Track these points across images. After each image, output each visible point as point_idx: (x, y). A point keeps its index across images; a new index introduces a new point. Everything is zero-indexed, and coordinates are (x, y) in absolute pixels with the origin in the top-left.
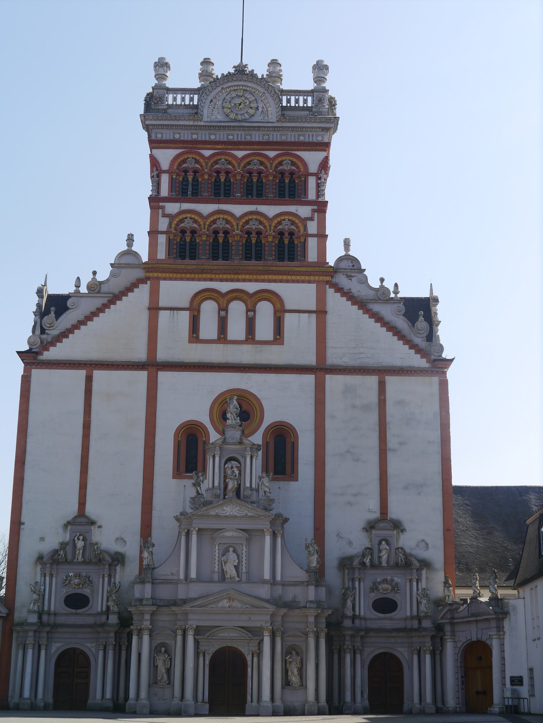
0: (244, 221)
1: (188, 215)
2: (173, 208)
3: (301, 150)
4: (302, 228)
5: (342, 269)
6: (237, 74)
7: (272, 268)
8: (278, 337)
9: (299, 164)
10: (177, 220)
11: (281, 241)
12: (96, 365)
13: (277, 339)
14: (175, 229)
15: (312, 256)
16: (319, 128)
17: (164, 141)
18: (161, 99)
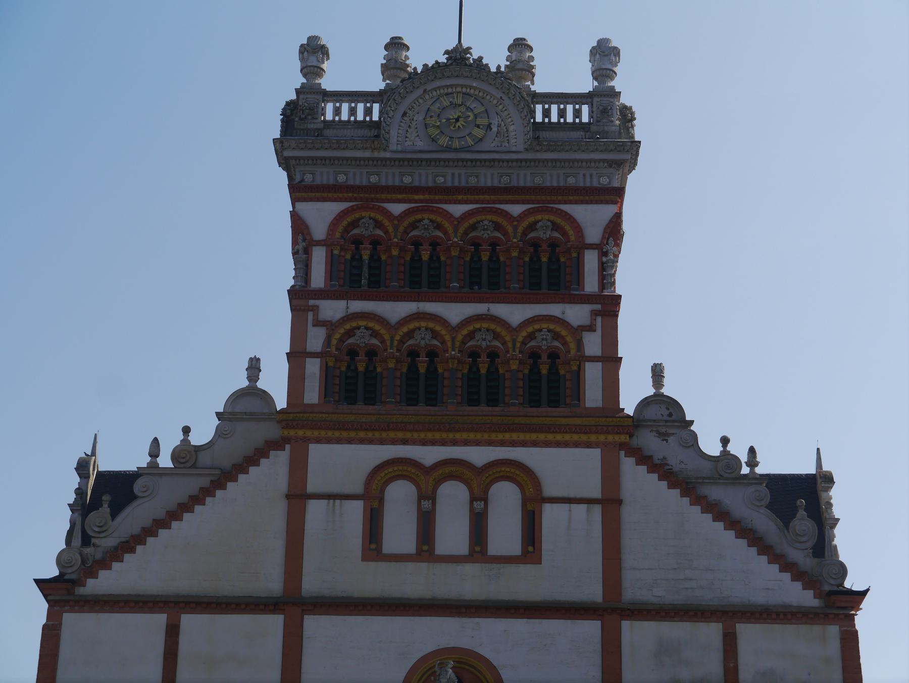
0: (465, 332)
1: (362, 323)
2: (333, 309)
3: (571, 202)
4: (572, 346)
5: (650, 421)
6: (451, 64)
7: (517, 420)
8: (530, 549)
9: (567, 228)
10: (342, 331)
11: (535, 369)
12: (187, 603)
13: (528, 552)
14: (337, 349)
15: (593, 396)
16: (604, 161)
17: (317, 186)
18: (315, 111)
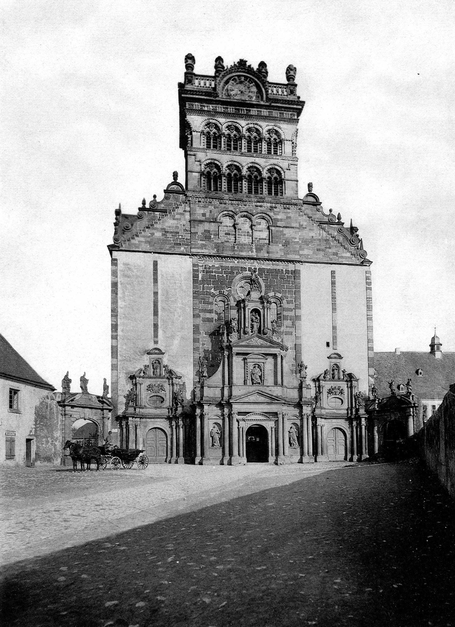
4: (283, 174)
